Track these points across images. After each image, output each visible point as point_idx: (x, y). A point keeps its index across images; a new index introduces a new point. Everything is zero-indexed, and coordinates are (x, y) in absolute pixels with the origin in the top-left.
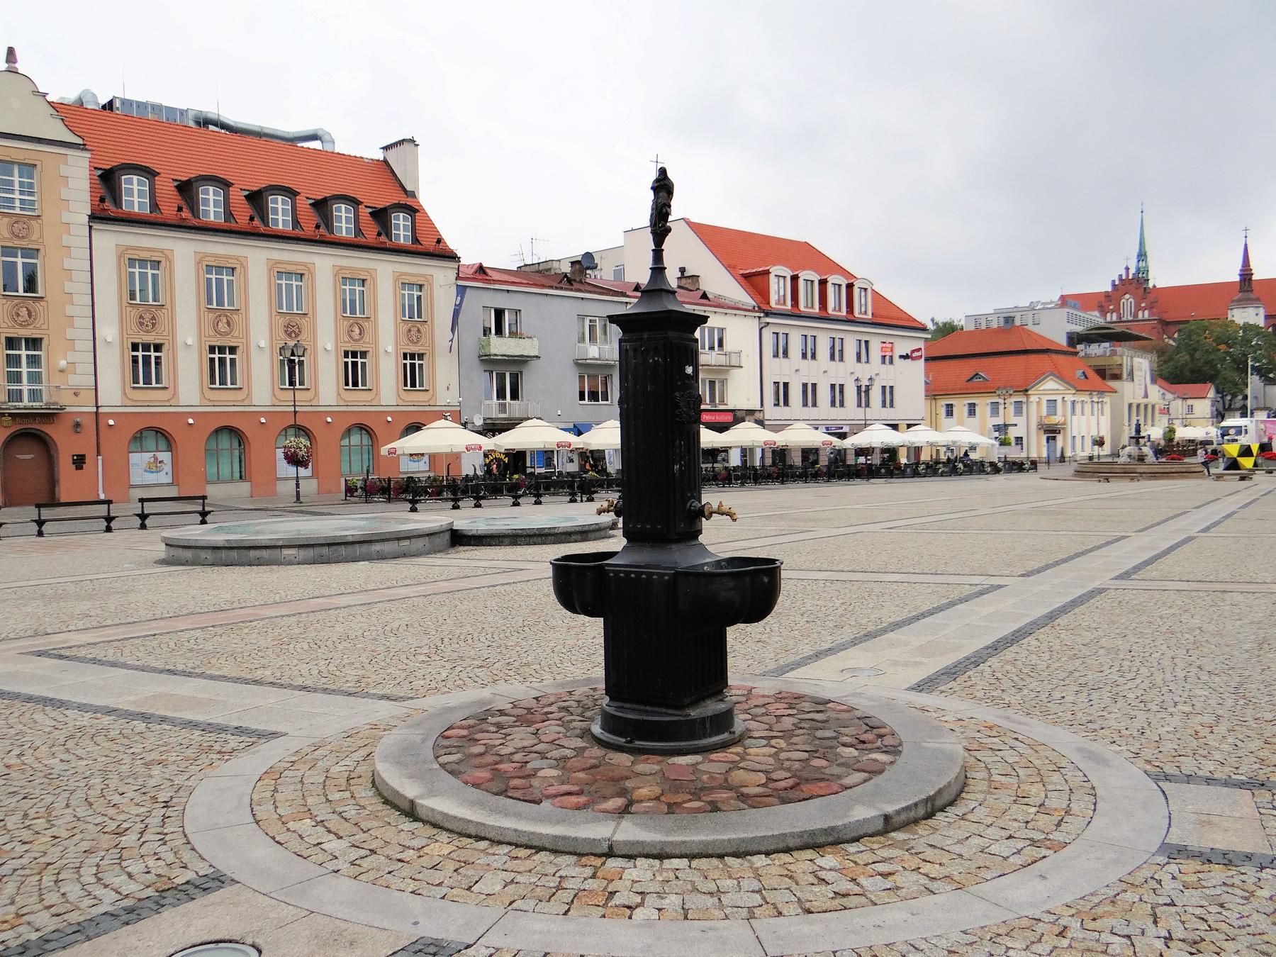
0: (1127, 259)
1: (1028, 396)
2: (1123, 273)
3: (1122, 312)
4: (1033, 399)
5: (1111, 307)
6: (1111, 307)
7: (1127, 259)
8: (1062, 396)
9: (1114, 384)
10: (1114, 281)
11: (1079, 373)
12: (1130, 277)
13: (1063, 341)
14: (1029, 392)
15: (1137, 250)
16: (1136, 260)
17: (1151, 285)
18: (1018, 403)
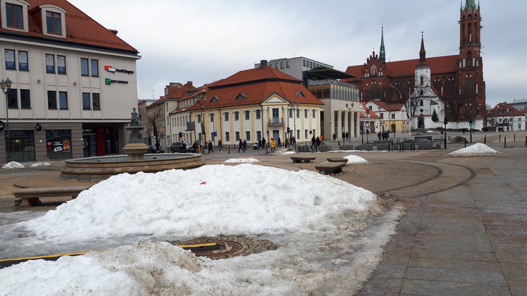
0: (374, 48)
1: (262, 106)
2: (372, 55)
3: (371, 73)
4: (265, 108)
5: (367, 71)
6: (367, 71)
7: (374, 48)
8: (282, 106)
9: (323, 101)
10: (368, 59)
11: (298, 93)
12: (375, 57)
13: (300, 77)
14: (262, 104)
15: (381, 45)
16: (380, 50)
17: (387, 61)
18: (258, 111)
